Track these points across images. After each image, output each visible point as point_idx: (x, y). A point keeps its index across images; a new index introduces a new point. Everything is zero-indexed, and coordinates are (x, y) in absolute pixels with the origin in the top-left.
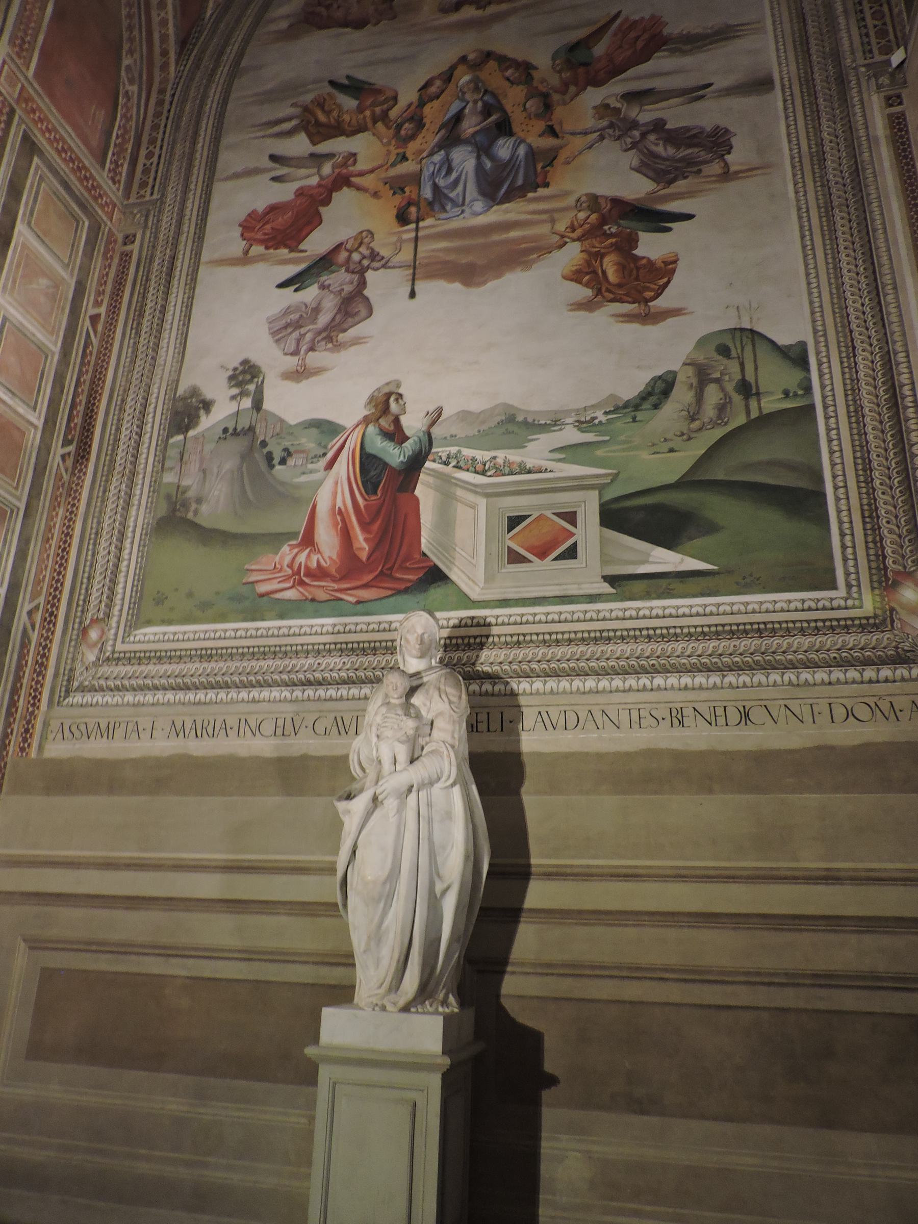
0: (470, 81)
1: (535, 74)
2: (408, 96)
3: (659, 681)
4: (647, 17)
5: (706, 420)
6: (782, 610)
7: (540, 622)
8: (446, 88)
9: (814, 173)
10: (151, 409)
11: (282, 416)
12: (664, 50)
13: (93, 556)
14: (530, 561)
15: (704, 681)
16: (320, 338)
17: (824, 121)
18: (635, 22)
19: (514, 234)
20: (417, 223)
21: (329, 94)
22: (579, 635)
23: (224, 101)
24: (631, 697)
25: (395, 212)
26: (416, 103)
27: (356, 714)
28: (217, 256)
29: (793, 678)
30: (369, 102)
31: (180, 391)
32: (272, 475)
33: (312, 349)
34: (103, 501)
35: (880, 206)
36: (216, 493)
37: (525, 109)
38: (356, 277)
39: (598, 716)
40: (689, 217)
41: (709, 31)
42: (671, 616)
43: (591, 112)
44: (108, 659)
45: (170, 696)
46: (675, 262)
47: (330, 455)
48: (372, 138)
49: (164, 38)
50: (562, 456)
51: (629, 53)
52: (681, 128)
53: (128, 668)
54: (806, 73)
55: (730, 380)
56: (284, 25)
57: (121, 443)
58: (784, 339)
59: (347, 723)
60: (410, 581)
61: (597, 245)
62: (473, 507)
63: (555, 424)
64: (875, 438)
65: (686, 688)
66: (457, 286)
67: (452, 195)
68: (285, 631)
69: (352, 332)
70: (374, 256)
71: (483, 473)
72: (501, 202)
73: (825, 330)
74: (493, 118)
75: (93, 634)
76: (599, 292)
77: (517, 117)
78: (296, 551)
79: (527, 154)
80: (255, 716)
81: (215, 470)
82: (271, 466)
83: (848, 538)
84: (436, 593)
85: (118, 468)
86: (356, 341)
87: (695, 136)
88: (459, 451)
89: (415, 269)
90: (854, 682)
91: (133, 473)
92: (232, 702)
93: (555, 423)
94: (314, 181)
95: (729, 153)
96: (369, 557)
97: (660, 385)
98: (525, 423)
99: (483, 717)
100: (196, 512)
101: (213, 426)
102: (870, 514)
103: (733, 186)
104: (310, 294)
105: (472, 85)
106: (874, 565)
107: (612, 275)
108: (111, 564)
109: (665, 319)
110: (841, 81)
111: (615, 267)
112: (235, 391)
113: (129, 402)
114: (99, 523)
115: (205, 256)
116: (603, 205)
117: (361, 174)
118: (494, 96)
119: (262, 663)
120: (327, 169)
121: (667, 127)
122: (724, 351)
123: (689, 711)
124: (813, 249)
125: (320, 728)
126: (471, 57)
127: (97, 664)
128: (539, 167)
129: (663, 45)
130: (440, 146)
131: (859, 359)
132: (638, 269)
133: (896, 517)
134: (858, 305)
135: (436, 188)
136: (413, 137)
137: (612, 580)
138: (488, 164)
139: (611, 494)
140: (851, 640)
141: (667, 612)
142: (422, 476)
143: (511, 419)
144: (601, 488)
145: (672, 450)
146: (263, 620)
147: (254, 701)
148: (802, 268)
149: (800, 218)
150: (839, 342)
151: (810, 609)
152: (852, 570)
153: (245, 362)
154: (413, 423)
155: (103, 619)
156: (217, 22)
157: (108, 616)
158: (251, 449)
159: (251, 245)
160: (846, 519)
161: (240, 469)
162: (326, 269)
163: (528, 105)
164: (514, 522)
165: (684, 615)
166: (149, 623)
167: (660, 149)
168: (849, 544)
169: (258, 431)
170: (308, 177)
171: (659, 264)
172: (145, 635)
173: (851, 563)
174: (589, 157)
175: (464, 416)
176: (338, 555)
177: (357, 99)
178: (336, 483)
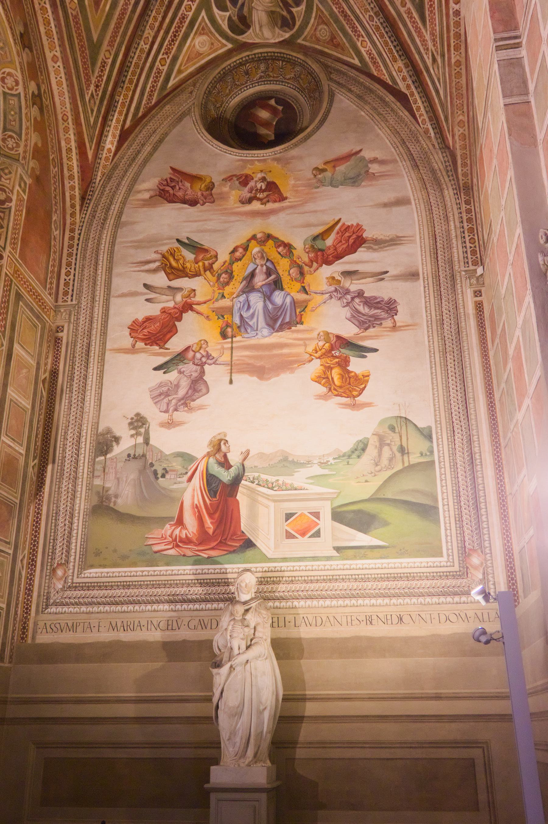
0: (259, 252)
1: (294, 251)
2: (224, 257)
3: (360, 601)
4: (355, 224)
5: (383, 466)
6: (418, 567)
7: (303, 570)
9: (438, 331)
10: (83, 439)
11: (161, 449)
12: (364, 247)
13: (55, 526)
14: (297, 538)
15: (381, 602)
16: (180, 403)
17: (443, 301)
18: (349, 226)
19: (285, 351)
20: (232, 338)
21: (177, 248)
22: (322, 578)
23: (113, 244)
24: (347, 610)
25: (219, 330)
26: (228, 261)
27: (210, 618)
28: (116, 346)
29: (423, 601)
31: (100, 430)
32: (158, 484)
33: (176, 410)
34: (58, 494)
35: (469, 354)
36: (126, 492)
37: (289, 275)
38: (199, 368)
39: (332, 619)
40: (376, 350)
41: (388, 238)
42: (366, 569)
43: (325, 281)
44: (70, 587)
45: (107, 608)
46: (368, 376)
47: (189, 474)
48: (204, 281)
49: (72, 197)
50: (312, 481)
51: (345, 246)
52: (372, 297)
53: (82, 592)
54: (435, 271)
55: (395, 445)
56: (146, 196)
57: (66, 459)
58: (421, 424)
59: (206, 623)
60: (236, 546)
61: (328, 361)
62: (267, 507)
63: (308, 463)
64: (462, 480)
65: (373, 605)
66: (255, 379)
67: (251, 323)
68: (170, 572)
69: (198, 402)
70: (208, 356)
71: (272, 489)
72: (277, 331)
73: (440, 421)
74: (273, 277)
75: (60, 572)
76: (330, 389)
77: (285, 279)
78: (173, 528)
79: (291, 303)
80: (156, 619)
81: (125, 479)
82: (157, 478)
83: (448, 531)
84: (250, 553)
85: (66, 475)
86: (201, 408)
87: (379, 303)
88: (259, 476)
89: (231, 366)
90: (450, 603)
91: (76, 478)
92: (143, 611)
93: (309, 462)
94: (171, 304)
95: (396, 314)
96: (214, 533)
97: (361, 446)
98: (293, 462)
99: (275, 620)
100: (115, 503)
101: (122, 452)
102: (459, 519)
103: (398, 334)
104: (173, 376)
105: (259, 255)
106: (460, 545)
107: (337, 381)
108: (67, 531)
109: (363, 408)
110: (453, 277)
111: (338, 376)
112: (133, 432)
113: (70, 435)
114: (57, 507)
115: (109, 346)
116: (332, 339)
117: (198, 304)
118: (273, 263)
119: (158, 590)
120: (179, 298)
121: (365, 295)
122: (392, 428)
123: (374, 617)
124: (436, 375)
125: (192, 626)
126: (259, 236)
127: (63, 589)
128: (298, 311)
130: (243, 292)
131: (456, 437)
132: (350, 378)
133: (471, 521)
134: (457, 408)
135: (241, 316)
136: (227, 284)
137: (338, 549)
138: (270, 306)
139: (337, 503)
140: (449, 582)
141: (364, 566)
142: (240, 489)
143: (285, 459)
144: (332, 500)
145: (366, 481)
146: (158, 566)
147: (155, 611)
148: (430, 385)
149: (430, 357)
150: (447, 428)
151: (430, 567)
152: (450, 547)
153: (138, 415)
154: (234, 458)
155: (64, 564)
156: (104, 187)
157: (67, 562)
158: (145, 467)
159: (136, 341)
160: (448, 522)
161: (139, 479)
162: (182, 361)
163: (291, 271)
164: (289, 516)
165: (372, 568)
166: (92, 566)
167: (361, 308)
168: (449, 534)
169: (148, 457)
170: (167, 301)
171: (361, 377)
172: (91, 573)
173: (450, 544)
174: (324, 309)
175: (261, 455)
176: (197, 531)
177: (194, 254)
178: (194, 490)
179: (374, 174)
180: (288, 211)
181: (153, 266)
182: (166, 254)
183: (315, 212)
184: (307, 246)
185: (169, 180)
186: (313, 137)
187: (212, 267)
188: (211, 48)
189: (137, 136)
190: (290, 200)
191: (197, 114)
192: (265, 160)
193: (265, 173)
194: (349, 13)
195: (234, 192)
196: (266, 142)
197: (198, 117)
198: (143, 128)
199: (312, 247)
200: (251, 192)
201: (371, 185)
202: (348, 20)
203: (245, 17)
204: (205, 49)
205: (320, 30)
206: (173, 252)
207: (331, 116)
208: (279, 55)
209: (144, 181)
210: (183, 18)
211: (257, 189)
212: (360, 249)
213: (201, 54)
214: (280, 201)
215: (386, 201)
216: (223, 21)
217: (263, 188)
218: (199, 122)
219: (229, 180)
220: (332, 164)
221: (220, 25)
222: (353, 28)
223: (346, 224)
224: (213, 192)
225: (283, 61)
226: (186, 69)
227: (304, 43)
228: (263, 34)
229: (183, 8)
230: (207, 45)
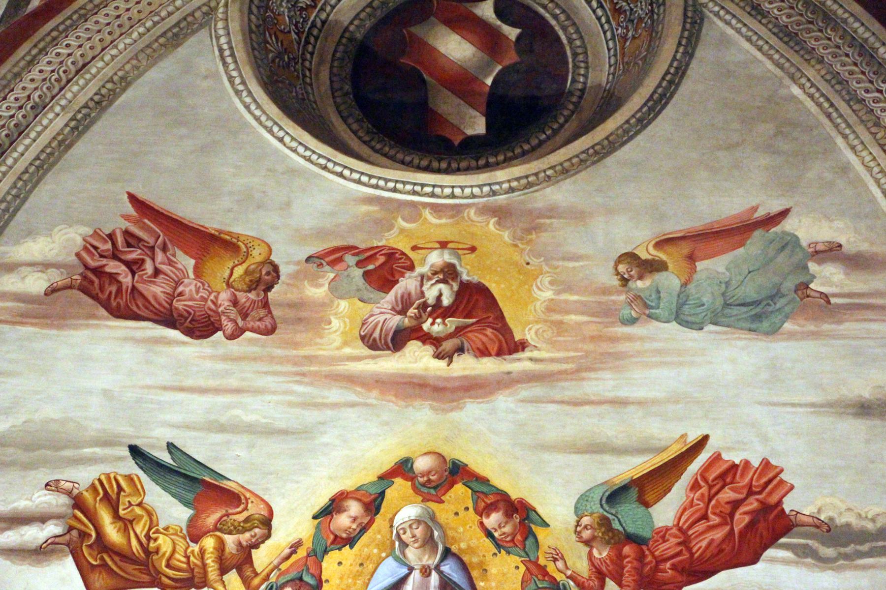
0: (418, 521)
1: (540, 533)
4: (756, 463)
8: (371, 522)
12: (786, 547)
18: (734, 467)
21: (129, 478)
26: (308, 544)
30: (211, 520)
41: (870, 526)
51: (718, 535)
105: (419, 532)
118: (464, 567)
126: (422, 464)
129: (782, 535)
177: (186, 504)
179: (825, 297)
180: (525, 392)
181: (35, 534)
182: (88, 496)
183: (622, 403)
184: (586, 520)
185: (120, 239)
186: (626, 152)
187: (249, 560)
189: (18, 76)
190: (535, 354)
191: (235, 26)
192: (457, 210)
193: (455, 252)
195: (343, 305)
196: (457, 140)
197: (237, 39)
198: (43, 51)
199: (605, 522)
200: (403, 312)
201: (816, 335)
206: (113, 491)
207: (686, 87)
209: (30, 233)
211: (425, 305)
212: (771, 552)
214: (499, 354)
215: (866, 393)
217: (446, 301)
218: (241, 54)
219: (332, 264)
220: (685, 248)
223: (725, 456)
224: (271, 295)
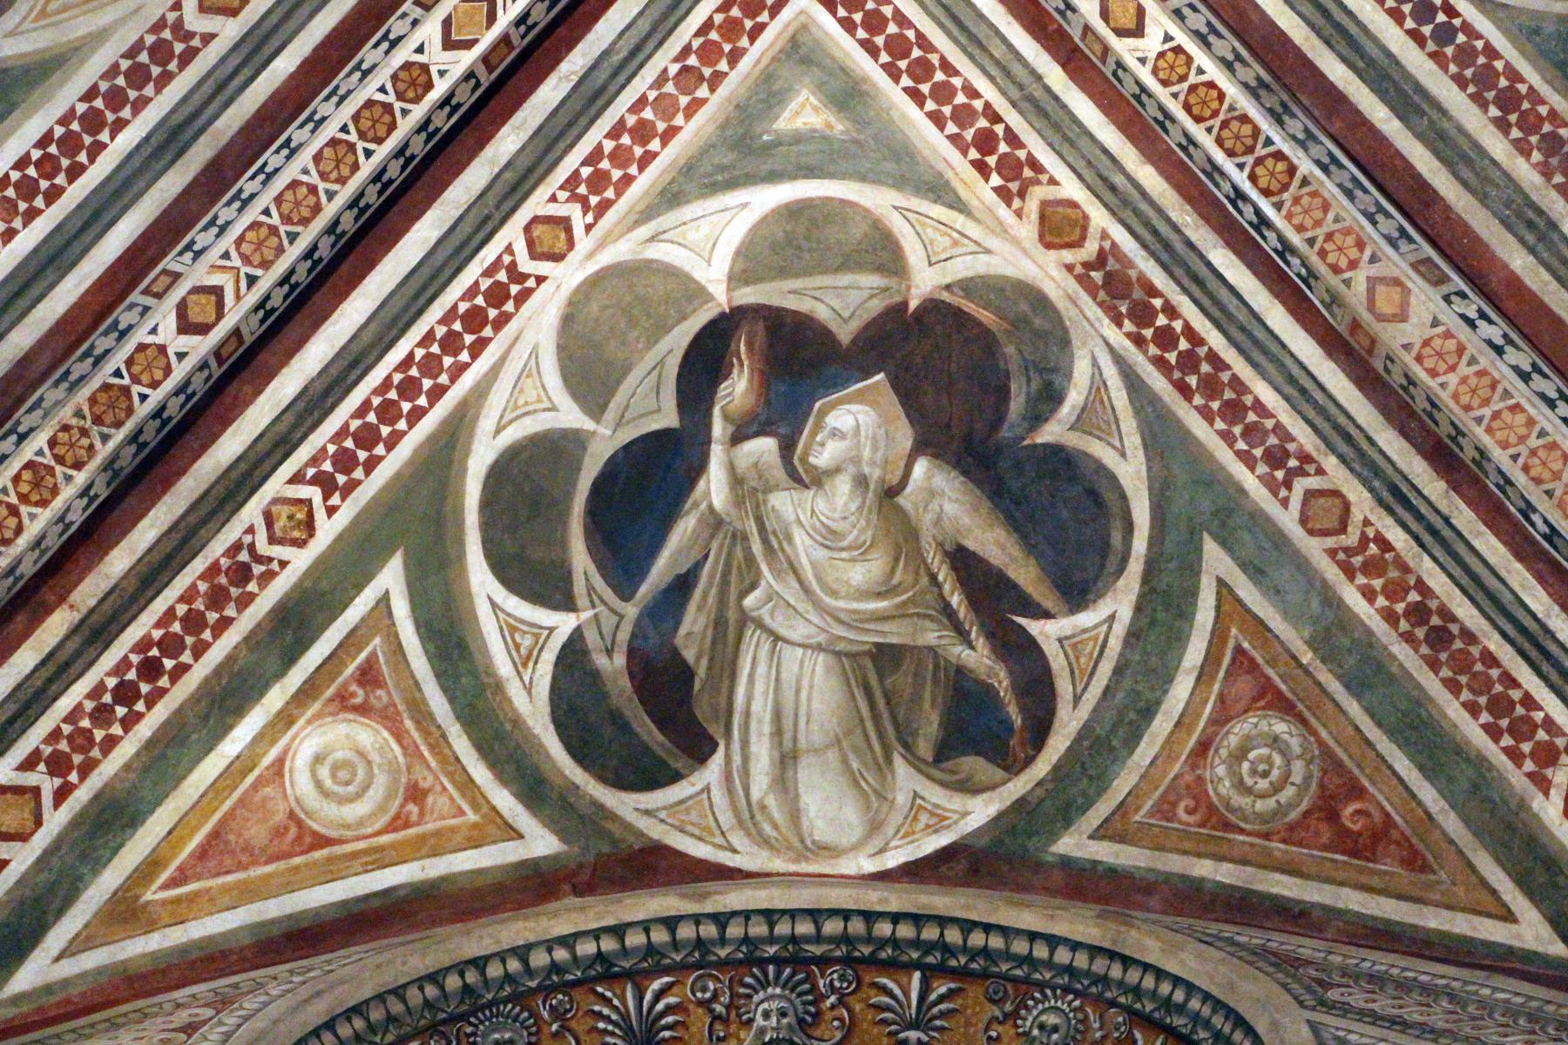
188: (399, 822)
194: (1465, 611)
202: (1462, 663)
203: (688, 674)
204: (360, 809)
205: (1241, 753)
208: (905, 931)
210: (241, 574)
213: (322, 841)
216: (525, 660)
221: (499, 687)
222: (1500, 706)
225: (930, 973)
226: (179, 912)
227: (1107, 853)
228: (795, 815)
229: (252, 512)
230: (376, 793)
